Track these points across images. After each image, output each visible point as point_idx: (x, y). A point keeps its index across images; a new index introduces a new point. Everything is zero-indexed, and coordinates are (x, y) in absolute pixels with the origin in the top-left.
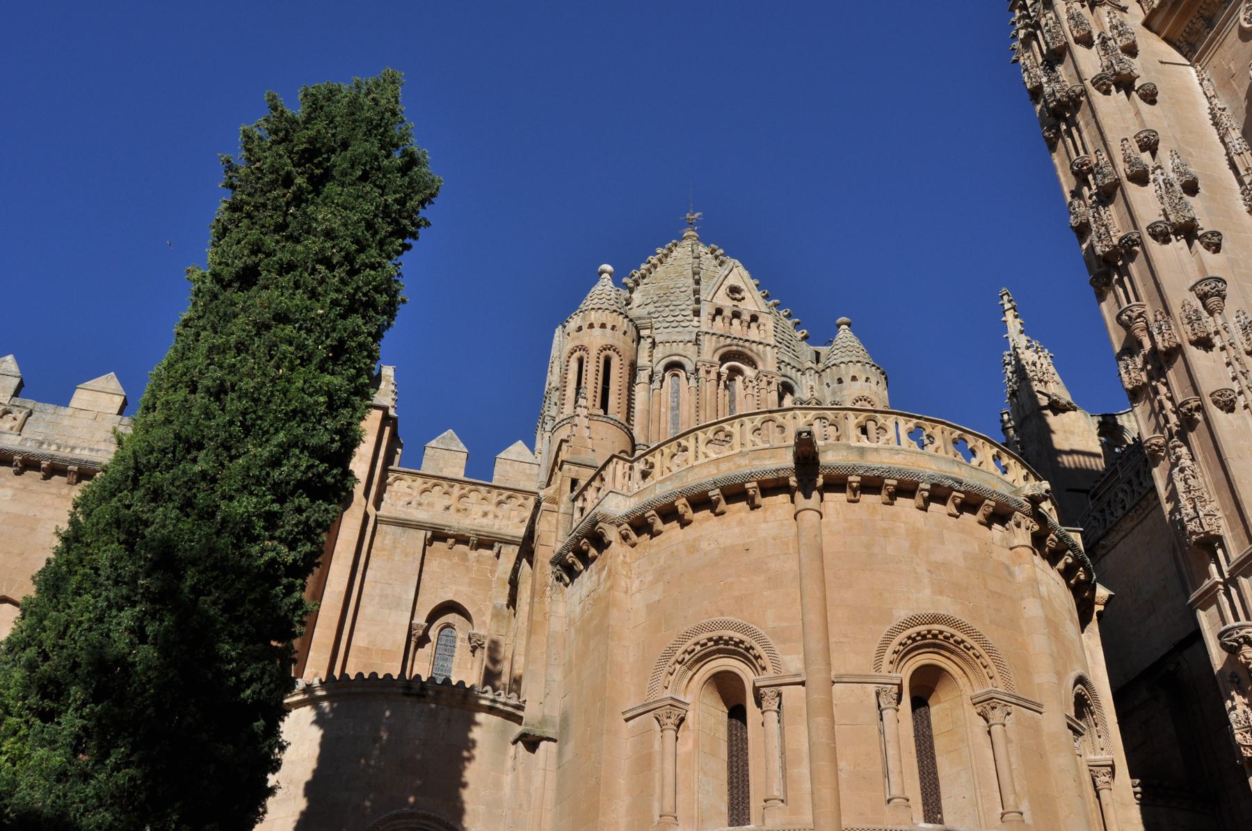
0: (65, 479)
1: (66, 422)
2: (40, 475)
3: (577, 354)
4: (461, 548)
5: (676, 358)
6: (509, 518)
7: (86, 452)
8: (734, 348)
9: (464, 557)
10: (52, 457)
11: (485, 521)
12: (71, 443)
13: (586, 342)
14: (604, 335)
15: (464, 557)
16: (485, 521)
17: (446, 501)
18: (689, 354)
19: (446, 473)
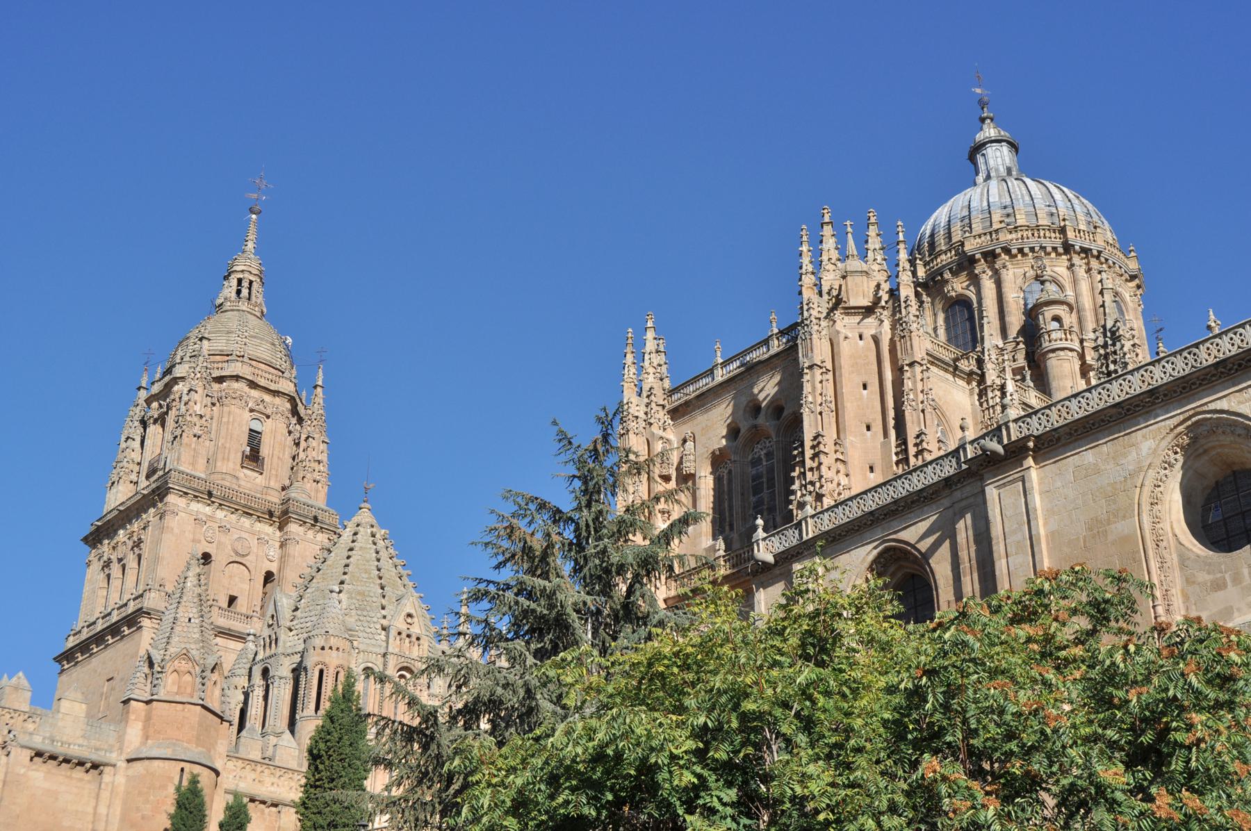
0: (69, 765)
1: (60, 724)
2: (55, 763)
3: (320, 667)
4: (262, 806)
5: (370, 665)
6: (283, 786)
7: (76, 747)
8: (405, 664)
9: (263, 812)
10: (66, 755)
11: (272, 789)
12: (65, 739)
13: (327, 661)
14: (338, 657)
15: (263, 812)
16: (272, 789)
17: (253, 775)
18: (378, 663)
19: (251, 757)
